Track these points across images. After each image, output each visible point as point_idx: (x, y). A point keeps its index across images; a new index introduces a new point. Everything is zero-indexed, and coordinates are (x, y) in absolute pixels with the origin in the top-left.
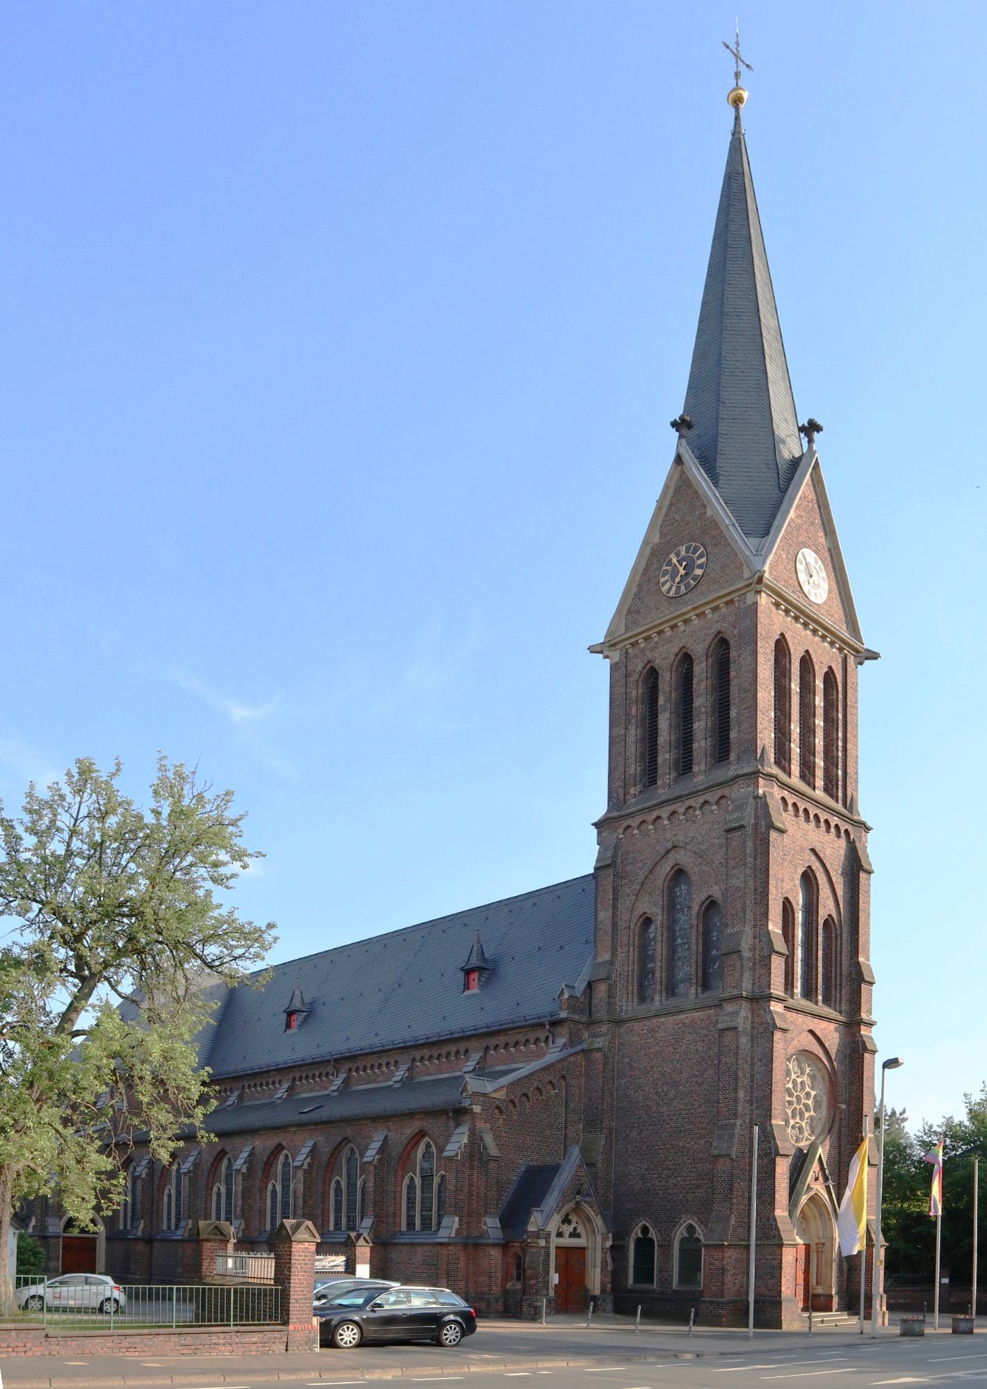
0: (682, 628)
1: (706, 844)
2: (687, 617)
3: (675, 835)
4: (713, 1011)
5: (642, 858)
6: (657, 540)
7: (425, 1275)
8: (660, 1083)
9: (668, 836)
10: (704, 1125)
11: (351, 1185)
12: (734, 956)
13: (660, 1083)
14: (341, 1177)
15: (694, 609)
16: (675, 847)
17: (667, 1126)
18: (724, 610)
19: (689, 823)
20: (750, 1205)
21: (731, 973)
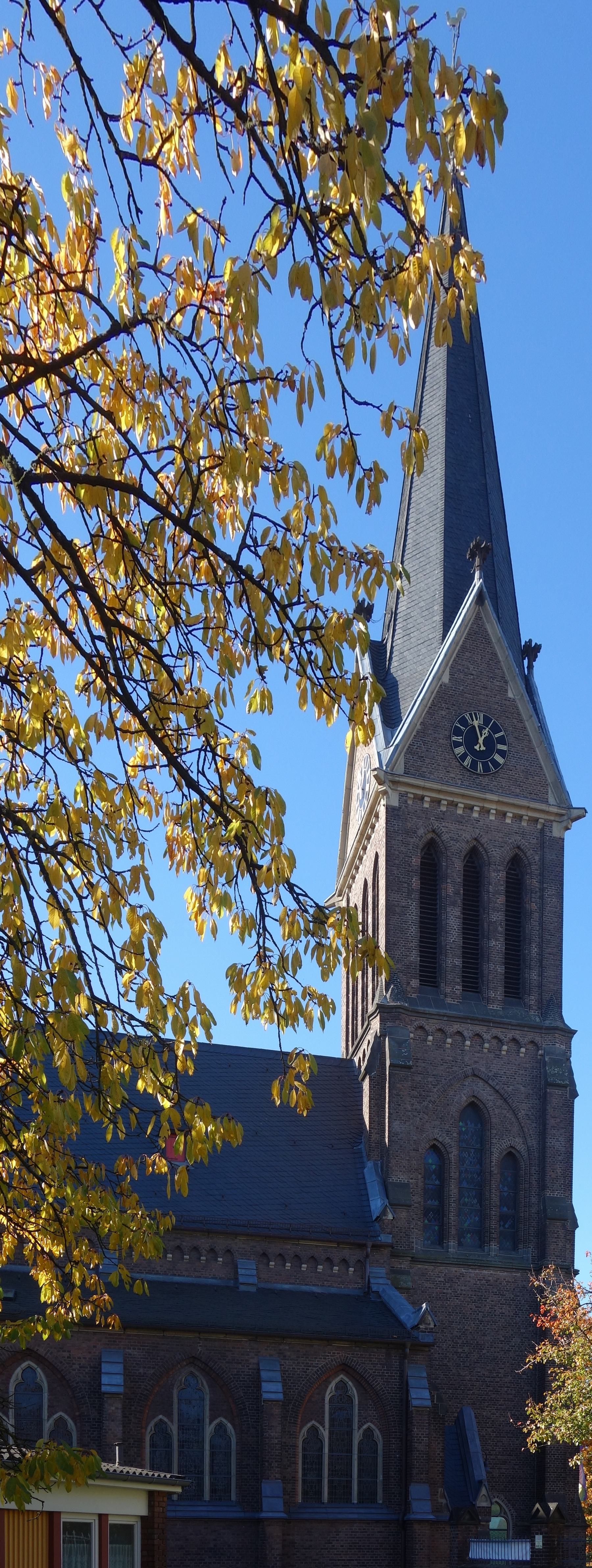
0: (475, 815)
1: (511, 1087)
2: (487, 805)
3: (476, 1062)
4: (519, 1275)
5: (434, 1073)
6: (446, 679)
7: (355, 1562)
8: (460, 1341)
9: (466, 1059)
10: (511, 1397)
11: (341, 1438)
12: (558, 1223)
13: (460, 1341)
14: (169, 1415)
15: (498, 802)
16: (475, 1075)
17: (469, 1392)
18: (524, 824)
19: (492, 1055)
20: (212, 1466)
21: (554, 1240)
